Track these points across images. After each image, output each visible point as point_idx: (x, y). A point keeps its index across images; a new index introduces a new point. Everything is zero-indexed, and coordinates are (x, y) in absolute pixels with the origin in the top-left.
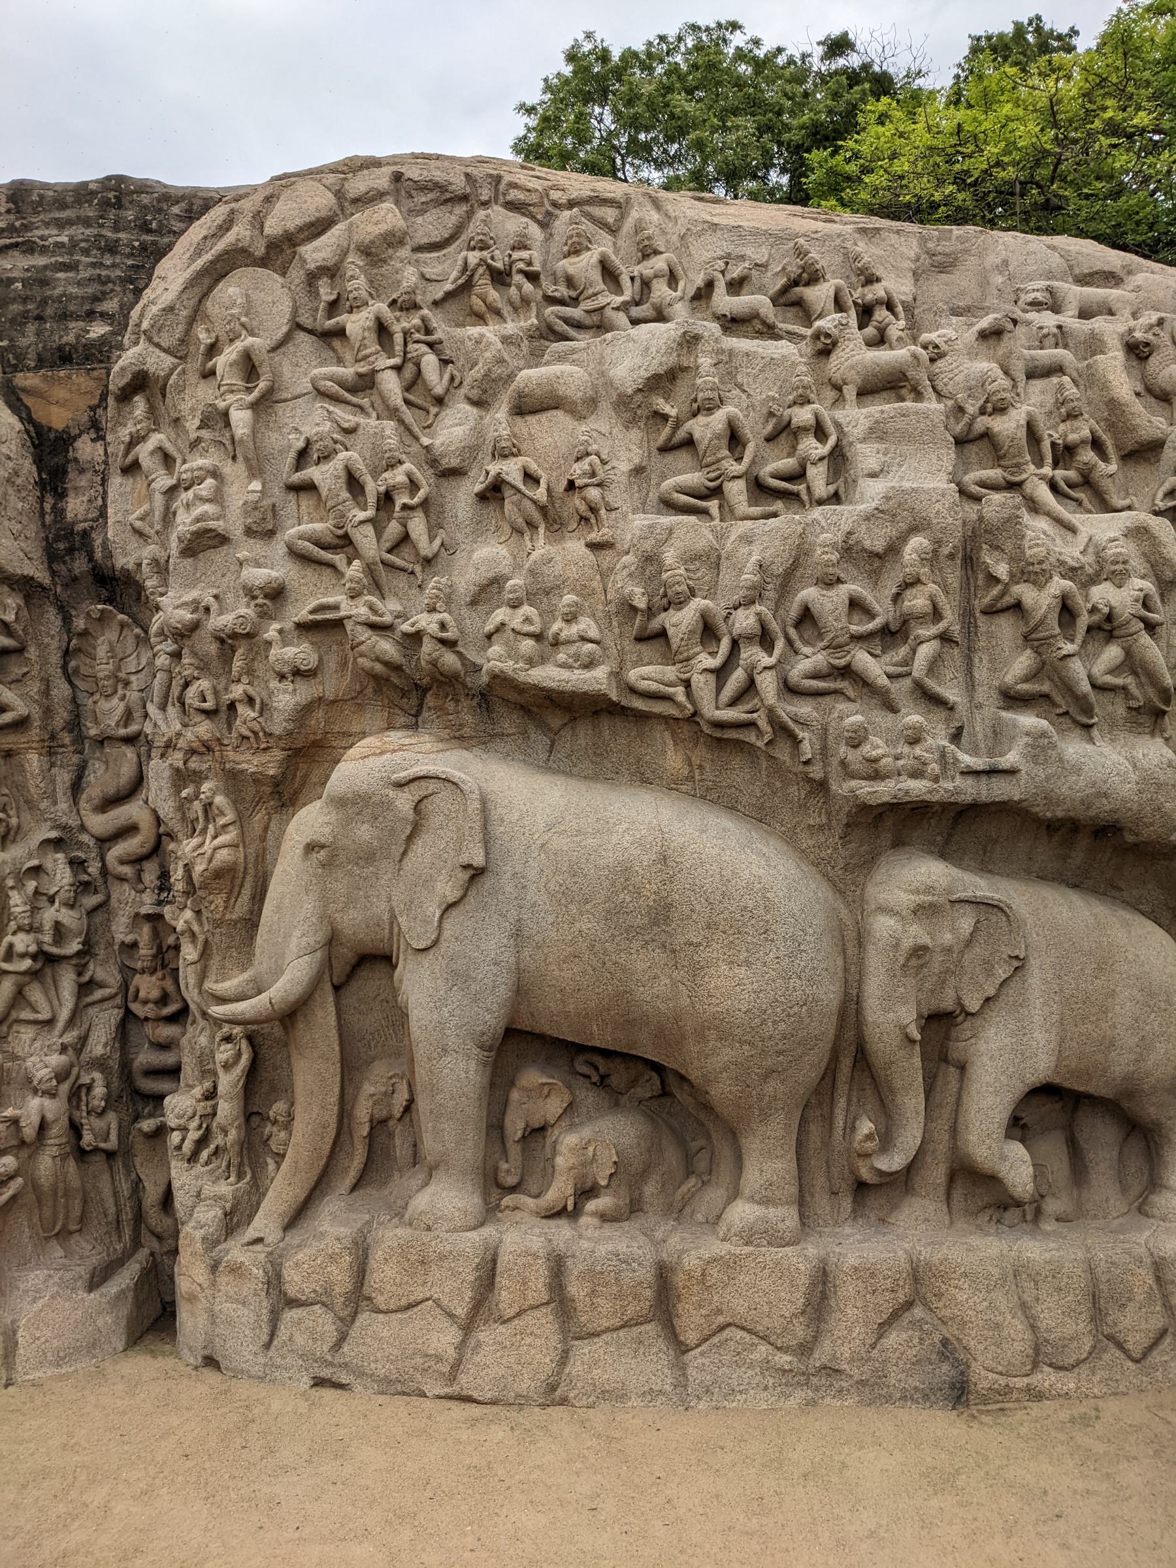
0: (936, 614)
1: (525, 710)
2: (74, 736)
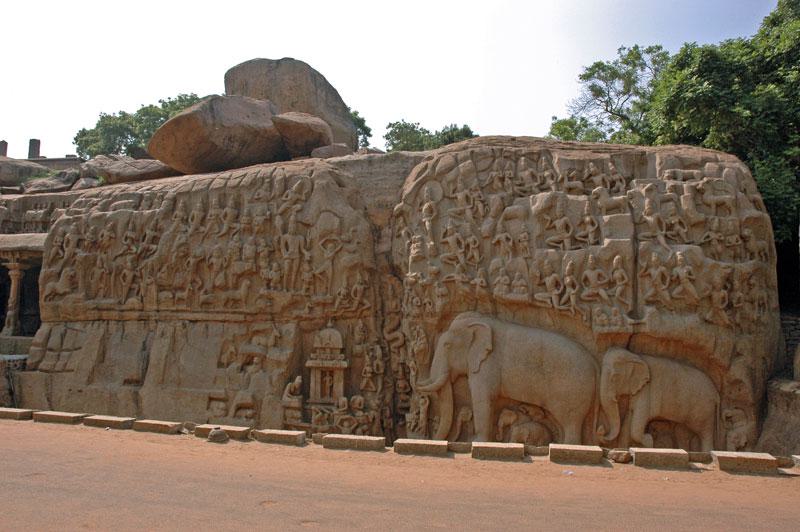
0: (623, 278)
2: (381, 312)
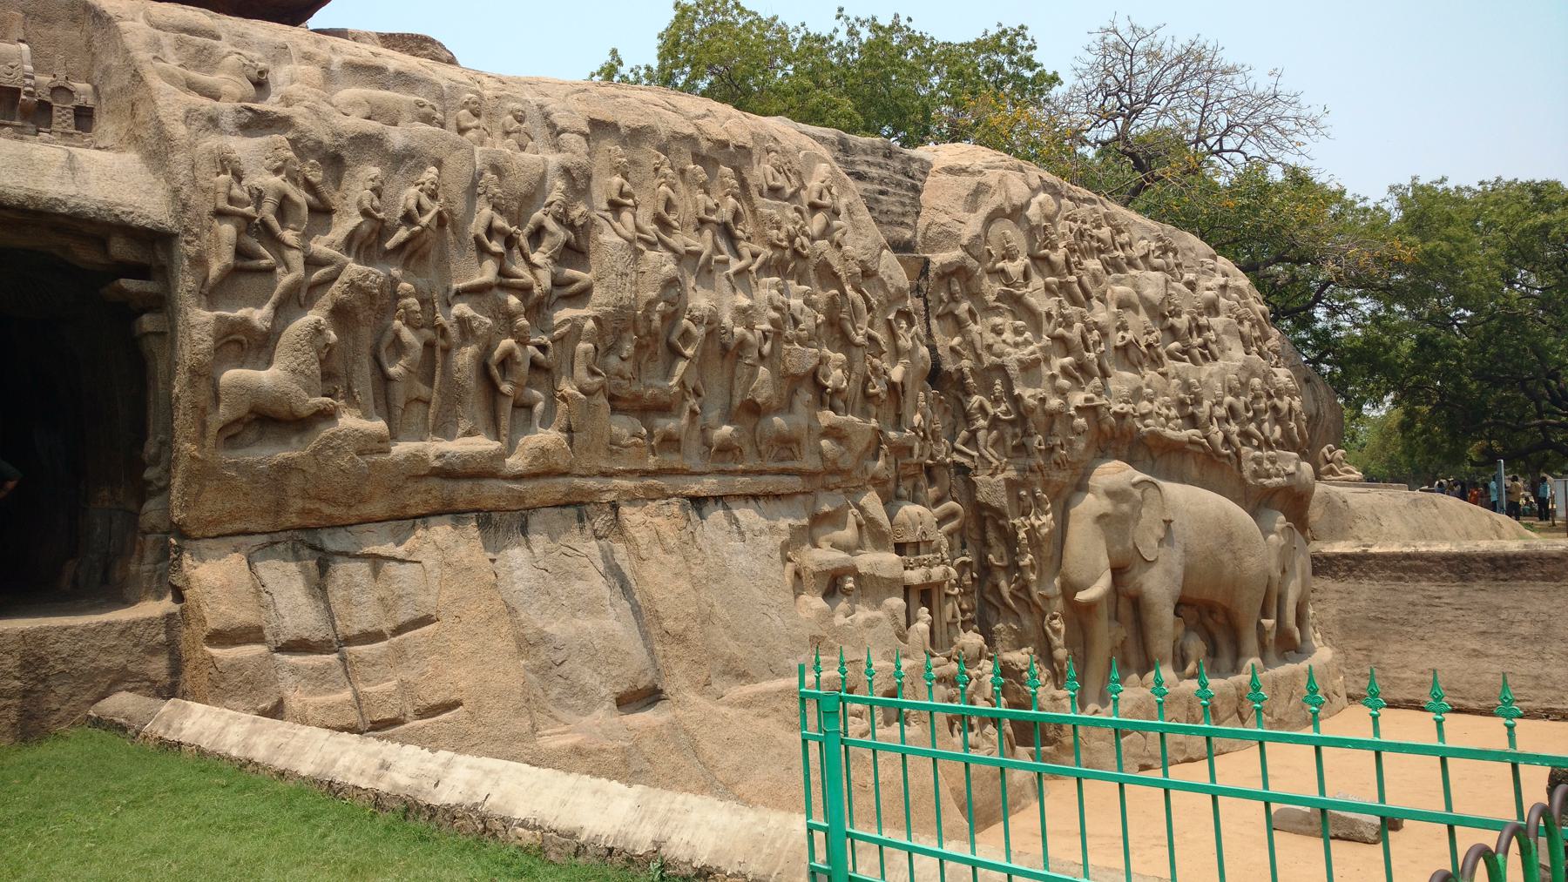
1: (1149, 449)
